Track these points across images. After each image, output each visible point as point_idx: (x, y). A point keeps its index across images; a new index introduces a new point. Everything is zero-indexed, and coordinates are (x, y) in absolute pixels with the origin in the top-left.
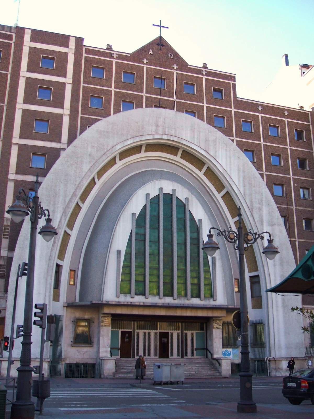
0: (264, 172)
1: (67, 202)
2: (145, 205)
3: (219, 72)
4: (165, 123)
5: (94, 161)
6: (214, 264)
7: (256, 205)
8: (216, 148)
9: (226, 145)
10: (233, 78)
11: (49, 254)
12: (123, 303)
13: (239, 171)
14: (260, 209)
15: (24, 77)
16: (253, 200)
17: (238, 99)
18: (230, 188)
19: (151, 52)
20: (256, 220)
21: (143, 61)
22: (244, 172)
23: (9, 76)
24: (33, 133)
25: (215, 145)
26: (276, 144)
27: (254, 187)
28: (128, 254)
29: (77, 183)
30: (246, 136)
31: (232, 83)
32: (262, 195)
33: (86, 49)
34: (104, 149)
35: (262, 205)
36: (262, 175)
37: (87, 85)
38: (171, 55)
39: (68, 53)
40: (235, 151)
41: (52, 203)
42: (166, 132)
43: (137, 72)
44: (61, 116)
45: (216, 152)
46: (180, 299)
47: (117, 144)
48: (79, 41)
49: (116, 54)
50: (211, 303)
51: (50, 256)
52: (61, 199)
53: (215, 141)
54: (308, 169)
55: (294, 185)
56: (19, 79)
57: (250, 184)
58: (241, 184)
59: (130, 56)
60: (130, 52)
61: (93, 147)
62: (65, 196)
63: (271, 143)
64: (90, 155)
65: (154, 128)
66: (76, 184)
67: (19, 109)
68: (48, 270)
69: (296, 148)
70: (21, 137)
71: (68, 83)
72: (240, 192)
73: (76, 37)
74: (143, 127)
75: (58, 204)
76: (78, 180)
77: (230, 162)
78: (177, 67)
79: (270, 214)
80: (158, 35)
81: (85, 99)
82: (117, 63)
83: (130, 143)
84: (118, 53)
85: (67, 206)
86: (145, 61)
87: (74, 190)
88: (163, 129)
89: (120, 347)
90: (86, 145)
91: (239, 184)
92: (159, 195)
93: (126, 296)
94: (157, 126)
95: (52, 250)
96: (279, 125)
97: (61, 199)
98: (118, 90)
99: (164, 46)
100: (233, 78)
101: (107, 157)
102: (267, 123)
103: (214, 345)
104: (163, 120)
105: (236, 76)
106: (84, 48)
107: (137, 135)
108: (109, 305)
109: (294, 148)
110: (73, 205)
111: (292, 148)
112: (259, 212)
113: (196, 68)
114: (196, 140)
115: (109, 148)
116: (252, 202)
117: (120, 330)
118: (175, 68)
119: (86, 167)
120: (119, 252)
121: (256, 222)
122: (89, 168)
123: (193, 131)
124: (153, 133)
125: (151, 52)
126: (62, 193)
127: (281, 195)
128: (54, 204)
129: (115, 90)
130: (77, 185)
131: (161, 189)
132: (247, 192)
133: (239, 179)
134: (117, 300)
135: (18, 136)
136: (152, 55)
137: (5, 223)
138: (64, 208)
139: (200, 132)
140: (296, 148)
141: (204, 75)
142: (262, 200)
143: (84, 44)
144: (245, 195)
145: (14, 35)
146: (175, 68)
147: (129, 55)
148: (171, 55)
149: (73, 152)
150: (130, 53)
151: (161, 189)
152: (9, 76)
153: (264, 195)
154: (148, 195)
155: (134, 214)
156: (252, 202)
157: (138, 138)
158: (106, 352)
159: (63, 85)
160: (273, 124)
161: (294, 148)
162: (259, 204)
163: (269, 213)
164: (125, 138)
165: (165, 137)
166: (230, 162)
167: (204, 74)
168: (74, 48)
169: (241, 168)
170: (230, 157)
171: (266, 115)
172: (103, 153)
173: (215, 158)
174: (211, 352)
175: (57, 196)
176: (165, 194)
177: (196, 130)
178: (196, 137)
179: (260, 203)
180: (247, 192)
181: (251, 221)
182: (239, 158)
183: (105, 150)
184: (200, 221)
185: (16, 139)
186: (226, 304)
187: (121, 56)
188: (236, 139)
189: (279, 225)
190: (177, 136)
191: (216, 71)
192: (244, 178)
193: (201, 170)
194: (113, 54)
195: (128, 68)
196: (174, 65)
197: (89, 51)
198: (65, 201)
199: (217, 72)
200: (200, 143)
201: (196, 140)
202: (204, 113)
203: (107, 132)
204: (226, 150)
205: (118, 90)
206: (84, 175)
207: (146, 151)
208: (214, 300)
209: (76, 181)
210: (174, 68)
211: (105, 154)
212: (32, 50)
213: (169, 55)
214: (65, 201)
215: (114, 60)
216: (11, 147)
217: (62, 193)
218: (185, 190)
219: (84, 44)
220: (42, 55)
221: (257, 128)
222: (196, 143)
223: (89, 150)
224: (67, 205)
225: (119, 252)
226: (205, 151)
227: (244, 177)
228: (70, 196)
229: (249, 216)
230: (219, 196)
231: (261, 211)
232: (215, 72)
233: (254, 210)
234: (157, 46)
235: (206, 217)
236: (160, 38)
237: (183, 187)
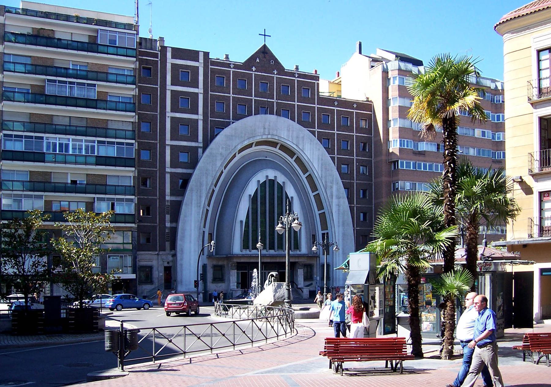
0: (336, 156)
1: (208, 189)
2: (257, 189)
3: (307, 74)
7: (329, 184)
8: (304, 143)
10: (317, 78)
11: (199, 226)
14: (331, 187)
15: (169, 90)
16: (327, 181)
17: (320, 96)
18: (312, 172)
19: (258, 60)
21: (252, 69)
22: (322, 160)
23: (159, 89)
25: (303, 140)
26: (346, 132)
27: (328, 171)
29: (214, 175)
31: (316, 82)
33: (211, 61)
34: (229, 149)
35: (333, 184)
36: (333, 159)
37: (213, 93)
38: (272, 62)
39: (198, 67)
41: (199, 190)
43: (248, 79)
44: (197, 120)
45: (304, 146)
47: (238, 145)
48: (206, 54)
49: (233, 64)
50: (298, 252)
52: (204, 187)
53: (303, 137)
54: (367, 151)
55: (356, 164)
56: (166, 92)
57: (326, 169)
58: (320, 169)
60: (243, 61)
61: (222, 148)
62: (207, 185)
63: (342, 132)
65: (262, 130)
67: (168, 117)
69: (360, 135)
70: (172, 139)
73: (203, 52)
74: (255, 131)
76: (214, 173)
77: (313, 153)
79: (338, 190)
81: (212, 105)
82: (233, 72)
83: (246, 143)
84: (233, 63)
85: (208, 193)
86: (254, 69)
87: (212, 181)
89: (240, 282)
90: (218, 147)
91: (318, 170)
92: (266, 181)
93: (246, 250)
94: (265, 128)
95: (201, 223)
97: (204, 187)
98: (235, 96)
100: (317, 78)
103: (299, 279)
105: (319, 76)
106: (210, 60)
108: (237, 256)
109: (358, 135)
110: (211, 190)
111: (357, 134)
114: (290, 137)
115: (233, 148)
116: (326, 182)
117: (240, 272)
118: (275, 73)
119: (219, 164)
120: (241, 222)
122: (220, 164)
123: (288, 130)
124: (262, 134)
125: (258, 60)
126: (205, 183)
129: (233, 95)
132: (323, 174)
133: (318, 165)
134: (241, 253)
135: (169, 139)
137: (167, 204)
139: (293, 131)
140: (360, 135)
141: (296, 78)
142: (333, 181)
143: (210, 57)
145: (159, 53)
146: (275, 73)
147: (242, 64)
148: (272, 62)
150: (243, 62)
151: (267, 176)
152: (159, 89)
153: (334, 176)
154: (259, 181)
155: (250, 195)
156: (326, 182)
158: (234, 285)
159: (197, 94)
161: (358, 135)
163: (337, 190)
165: (269, 136)
166: (313, 153)
167: (296, 76)
168: (203, 62)
169: (320, 157)
170: (313, 149)
172: (229, 151)
174: (297, 284)
176: (270, 180)
177: (290, 130)
179: (332, 183)
180: (323, 174)
182: (319, 149)
183: (231, 150)
184: (292, 198)
185: (168, 142)
186: (307, 253)
187: (237, 66)
188: (317, 130)
189: (344, 198)
191: (305, 73)
192: (322, 165)
194: (230, 64)
195: (242, 76)
197: (214, 63)
198: (207, 189)
199: (306, 74)
201: (290, 137)
202: (295, 111)
203: (232, 136)
204: (311, 144)
205: (235, 96)
208: (300, 251)
209: (213, 174)
210: (274, 73)
211: (230, 152)
212: (173, 65)
213: (271, 61)
214: (207, 189)
215: (232, 69)
216: (165, 148)
217: (205, 183)
218: (283, 176)
219: (210, 57)
220: (180, 70)
221: (333, 120)
222: (290, 140)
223: (220, 150)
225: (241, 222)
226: (297, 145)
228: (210, 185)
229: (324, 192)
230: (304, 177)
232: (304, 73)
233: (327, 188)
235: (296, 195)
237: (281, 174)
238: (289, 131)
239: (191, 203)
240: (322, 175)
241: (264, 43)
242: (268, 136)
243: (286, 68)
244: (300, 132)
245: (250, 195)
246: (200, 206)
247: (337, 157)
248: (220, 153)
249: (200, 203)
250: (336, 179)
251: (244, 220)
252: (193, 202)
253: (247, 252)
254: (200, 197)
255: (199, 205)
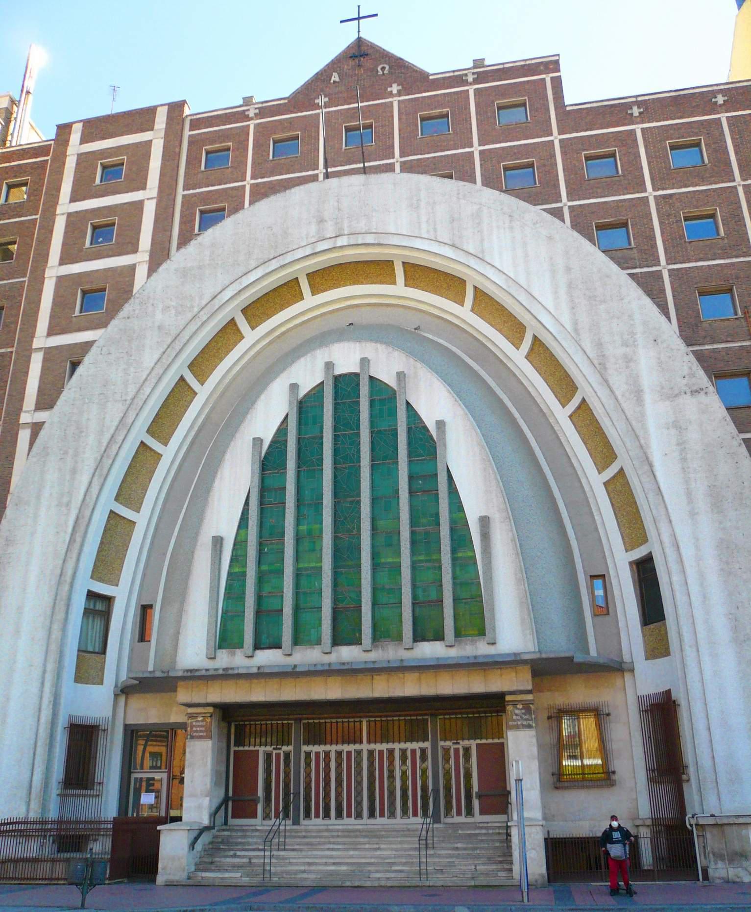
1: (105, 444)
4: (339, 209)
5: (169, 340)
6: (486, 536)
7: (615, 351)
8: (480, 232)
9: (510, 216)
11: (59, 571)
12: (203, 673)
13: (553, 272)
14: (628, 360)
17: (568, 108)
20: (618, 393)
21: (316, 101)
24: (74, 319)
27: (604, 301)
28: (239, 544)
30: (599, 191)
32: (633, 320)
34: (192, 307)
38: (383, 69)
40: (538, 225)
41: (71, 452)
42: (343, 230)
45: (482, 241)
46: (383, 650)
50: (481, 649)
51: (61, 575)
52: (91, 439)
53: (477, 216)
59: (289, 102)
60: (287, 93)
62: (101, 432)
64: (160, 328)
65: (313, 229)
66: (126, 400)
68: (54, 608)
71: (148, 199)
72: (563, 327)
75: (84, 452)
76: (132, 390)
77: (526, 255)
78: (400, 88)
80: (353, 37)
88: (336, 224)
92: (322, 383)
93: (234, 654)
94: (321, 221)
96: (701, 136)
97: (91, 439)
99: (367, 55)
101: (200, 323)
102: (665, 141)
104: (336, 204)
107: (272, 257)
112: (627, 367)
113: (452, 74)
116: (600, 345)
120: (218, 542)
121: (619, 397)
122: (156, 356)
123: (415, 207)
124: (313, 240)
127: (732, 316)
128: (76, 454)
130: (128, 402)
131: (329, 366)
134: (211, 665)
136: (338, 82)
138: (99, 458)
141: (471, 84)
142: (632, 334)
144: (576, 330)
147: (286, 101)
148: (383, 69)
149: (121, 330)
150: (287, 95)
151: (329, 366)
154: (294, 387)
155: (258, 441)
156: (600, 345)
157: (274, 261)
160: (683, 137)
162: (625, 344)
163: (660, 363)
164: (242, 269)
166: (526, 255)
171: (657, 121)
172: (190, 316)
173: (480, 256)
175: (83, 434)
176: (337, 379)
177: (423, 204)
178: (424, 219)
181: (604, 400)
182: (550, 238)
183: (196, 310)
184: (441, 424)
187: (265, 110)
190: (374, 231)
191: (503, 64)
192: (570, 286)
193: (464, 302)
196: (391, 86)
200: (435, 230)
201: (424, 226)
204: (511, 228)
206: (144, 377)
207: (315, 291)
213: (379, 69)
214: (100, 442)
223: (159, 316)
224: (105, 452)
225: (218, 542)
226: (453, 246)
227: (571, 283)
228: (112, 431)
231: (632, 364)
232: (501, 67)
234: (351, 62)
236: (359, 41)
238: (418, 207)
239: (38, 497)
240: (575, 323)
241: (357, 36)
242: (335, 243)
243: (431, 72)
244: (462, 201)
245: (258, 441)
246: (68, 505)
247: (669, 270)
248: (157, 324)
249: (70, 493)
250: (645, 323)
251: (229, 533)
252: (46, 493)
253: (238, 660)
254: (74, 471)
255: (65, 500)
